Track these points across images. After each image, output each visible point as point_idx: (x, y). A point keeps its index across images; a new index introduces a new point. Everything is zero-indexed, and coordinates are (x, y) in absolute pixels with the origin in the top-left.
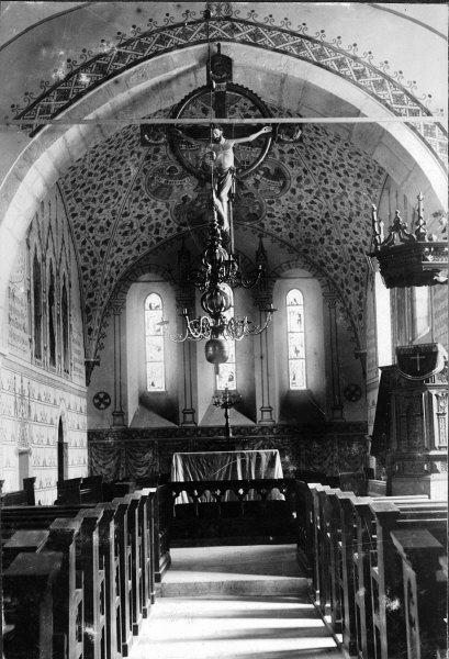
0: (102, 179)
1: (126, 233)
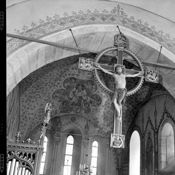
0: (37, 89)
1: (40, 112)
